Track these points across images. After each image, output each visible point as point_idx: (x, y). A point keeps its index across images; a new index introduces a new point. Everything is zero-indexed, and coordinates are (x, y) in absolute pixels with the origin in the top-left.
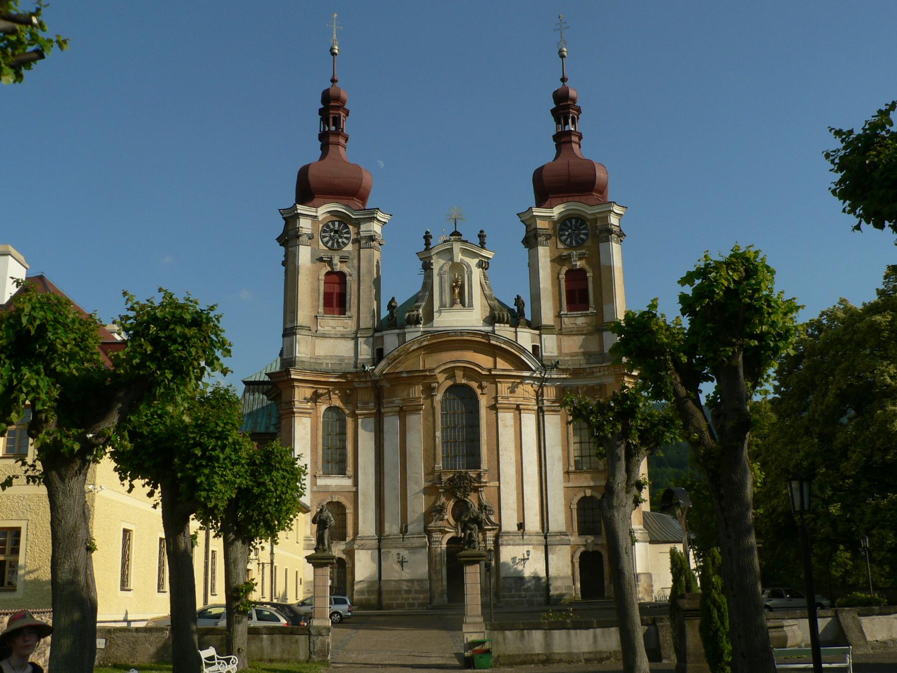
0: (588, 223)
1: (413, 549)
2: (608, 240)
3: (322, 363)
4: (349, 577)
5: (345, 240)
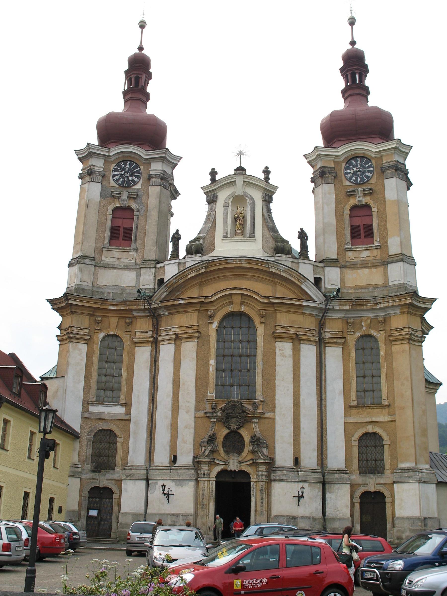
1: (180, 481)
3: (104, 292)
4: (115, 508)
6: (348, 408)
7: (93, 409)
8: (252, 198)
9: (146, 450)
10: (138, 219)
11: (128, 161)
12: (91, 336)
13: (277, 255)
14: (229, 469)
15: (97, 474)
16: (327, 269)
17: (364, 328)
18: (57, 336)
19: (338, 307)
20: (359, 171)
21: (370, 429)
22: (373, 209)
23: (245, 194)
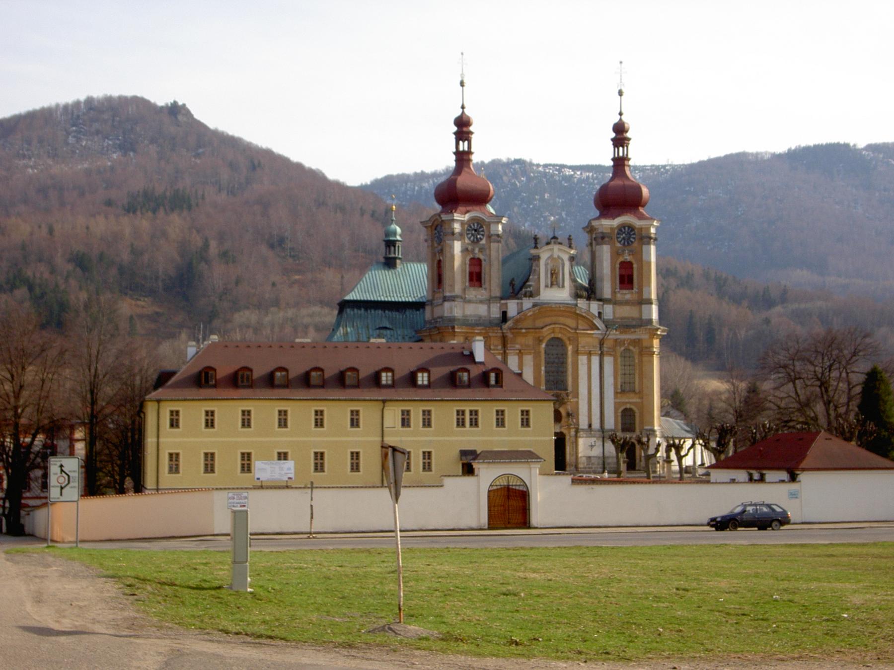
0: (636, 231)
2: (649, 244)
6: (616, 393)
16: (605, 306)
17: (626, 345)
21: (628, 406)
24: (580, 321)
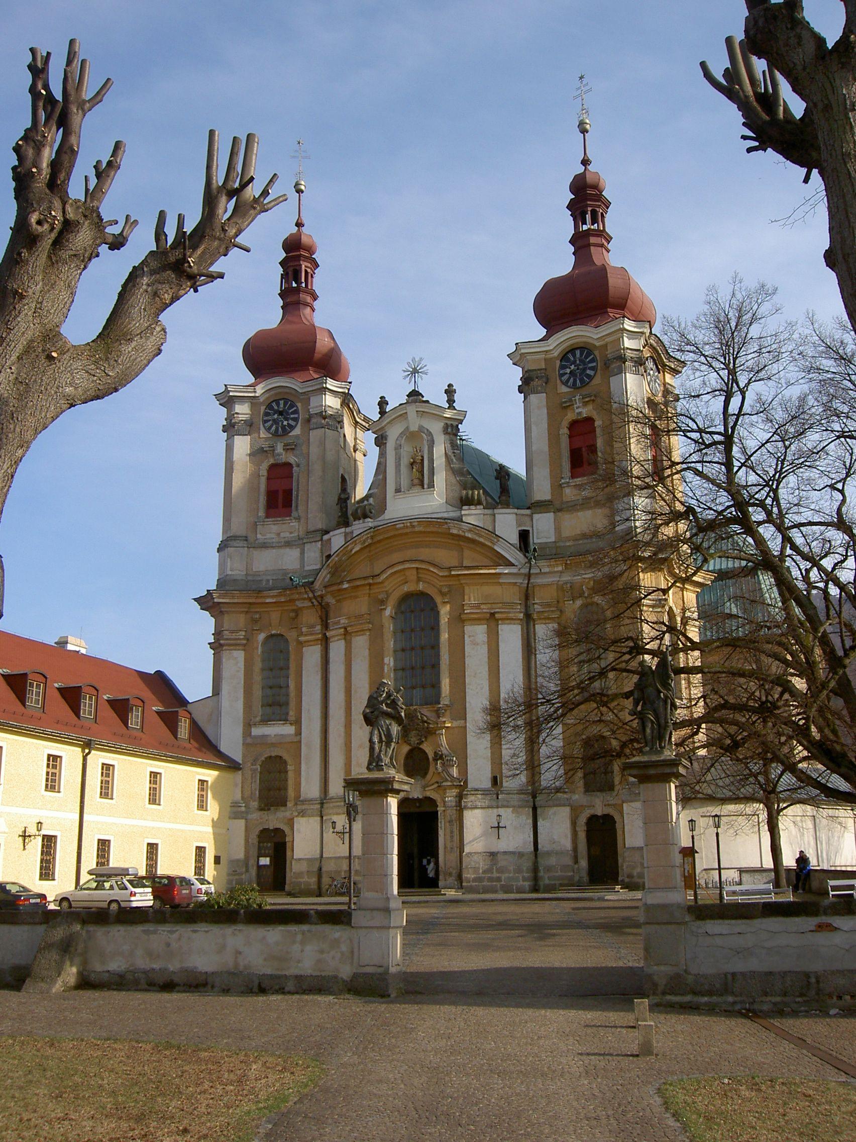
0: (597, 353)
2: (620, 371)
3: (262, 580)
5: (291, 422)
7: (256, 731)
8: (430, 432)
9: (321, 779)
10: (298, 477)
11: (281, 399)
12: (248, 640)
13: (464, 507)
14: (411, 797)
15: (265, 812)
16: (536, 516)
18: (209, 644)
19: (547, 570)
20: (578, 369)
22: (597, 424)
23: (421, 429)
24: (467, 553)
